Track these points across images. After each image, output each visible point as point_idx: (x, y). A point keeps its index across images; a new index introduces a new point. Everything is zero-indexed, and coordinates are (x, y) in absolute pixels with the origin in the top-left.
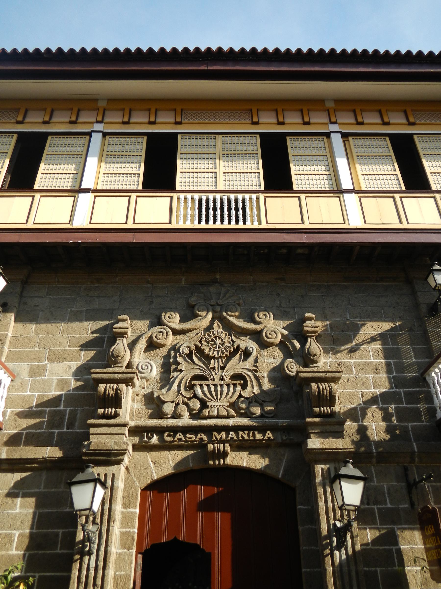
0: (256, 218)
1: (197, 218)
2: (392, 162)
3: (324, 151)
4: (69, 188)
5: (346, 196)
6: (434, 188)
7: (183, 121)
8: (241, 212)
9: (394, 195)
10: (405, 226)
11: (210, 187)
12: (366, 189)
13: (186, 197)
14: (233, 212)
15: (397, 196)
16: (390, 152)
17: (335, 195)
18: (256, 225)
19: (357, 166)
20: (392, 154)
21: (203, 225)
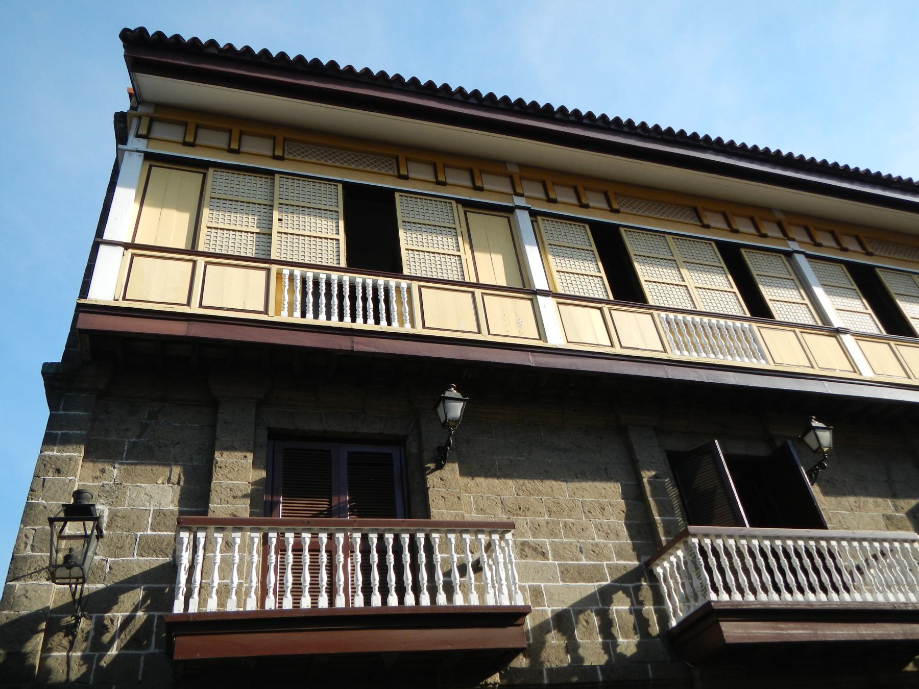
0: (408, 317)
1: (299, 306)
2: (594, 259)
3: (453, 221)
4: (183, 248)
5: (540, 299)
6: (651, 302)
7: (286, 156)
8: (382, 306)
9: (603, 305)
10: (617, 350)
11: (330, 261)
12: (563, 292)
13: (280, 272)
14: (335, 301)
15: (606, 308)
16: (591, 246)
17: (525, 296)
18: (407, 329)
19: (550, 257)
20: (594, 248)
21: (309, 319)
